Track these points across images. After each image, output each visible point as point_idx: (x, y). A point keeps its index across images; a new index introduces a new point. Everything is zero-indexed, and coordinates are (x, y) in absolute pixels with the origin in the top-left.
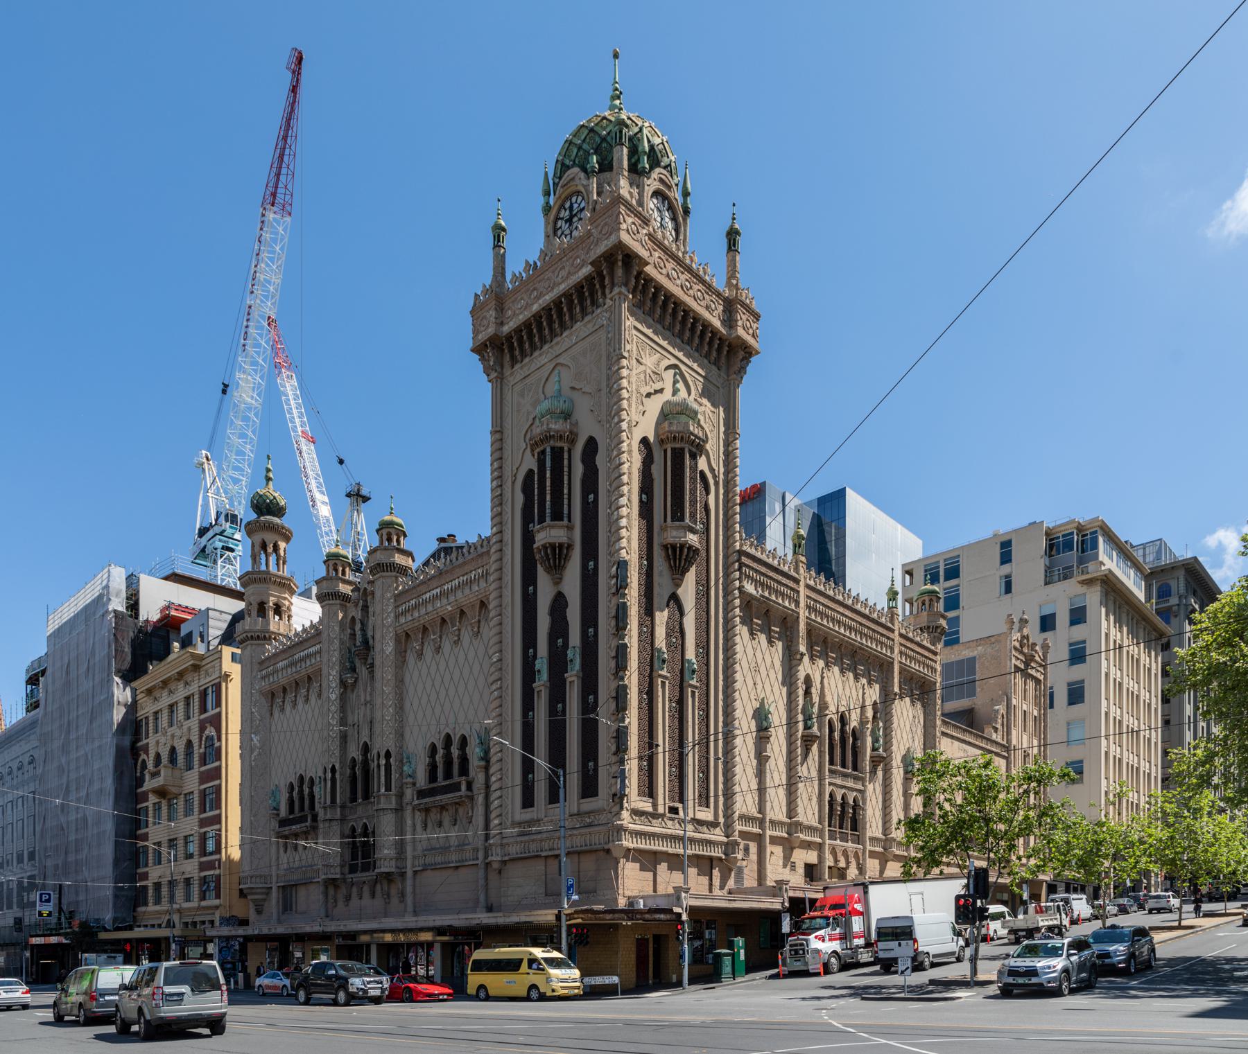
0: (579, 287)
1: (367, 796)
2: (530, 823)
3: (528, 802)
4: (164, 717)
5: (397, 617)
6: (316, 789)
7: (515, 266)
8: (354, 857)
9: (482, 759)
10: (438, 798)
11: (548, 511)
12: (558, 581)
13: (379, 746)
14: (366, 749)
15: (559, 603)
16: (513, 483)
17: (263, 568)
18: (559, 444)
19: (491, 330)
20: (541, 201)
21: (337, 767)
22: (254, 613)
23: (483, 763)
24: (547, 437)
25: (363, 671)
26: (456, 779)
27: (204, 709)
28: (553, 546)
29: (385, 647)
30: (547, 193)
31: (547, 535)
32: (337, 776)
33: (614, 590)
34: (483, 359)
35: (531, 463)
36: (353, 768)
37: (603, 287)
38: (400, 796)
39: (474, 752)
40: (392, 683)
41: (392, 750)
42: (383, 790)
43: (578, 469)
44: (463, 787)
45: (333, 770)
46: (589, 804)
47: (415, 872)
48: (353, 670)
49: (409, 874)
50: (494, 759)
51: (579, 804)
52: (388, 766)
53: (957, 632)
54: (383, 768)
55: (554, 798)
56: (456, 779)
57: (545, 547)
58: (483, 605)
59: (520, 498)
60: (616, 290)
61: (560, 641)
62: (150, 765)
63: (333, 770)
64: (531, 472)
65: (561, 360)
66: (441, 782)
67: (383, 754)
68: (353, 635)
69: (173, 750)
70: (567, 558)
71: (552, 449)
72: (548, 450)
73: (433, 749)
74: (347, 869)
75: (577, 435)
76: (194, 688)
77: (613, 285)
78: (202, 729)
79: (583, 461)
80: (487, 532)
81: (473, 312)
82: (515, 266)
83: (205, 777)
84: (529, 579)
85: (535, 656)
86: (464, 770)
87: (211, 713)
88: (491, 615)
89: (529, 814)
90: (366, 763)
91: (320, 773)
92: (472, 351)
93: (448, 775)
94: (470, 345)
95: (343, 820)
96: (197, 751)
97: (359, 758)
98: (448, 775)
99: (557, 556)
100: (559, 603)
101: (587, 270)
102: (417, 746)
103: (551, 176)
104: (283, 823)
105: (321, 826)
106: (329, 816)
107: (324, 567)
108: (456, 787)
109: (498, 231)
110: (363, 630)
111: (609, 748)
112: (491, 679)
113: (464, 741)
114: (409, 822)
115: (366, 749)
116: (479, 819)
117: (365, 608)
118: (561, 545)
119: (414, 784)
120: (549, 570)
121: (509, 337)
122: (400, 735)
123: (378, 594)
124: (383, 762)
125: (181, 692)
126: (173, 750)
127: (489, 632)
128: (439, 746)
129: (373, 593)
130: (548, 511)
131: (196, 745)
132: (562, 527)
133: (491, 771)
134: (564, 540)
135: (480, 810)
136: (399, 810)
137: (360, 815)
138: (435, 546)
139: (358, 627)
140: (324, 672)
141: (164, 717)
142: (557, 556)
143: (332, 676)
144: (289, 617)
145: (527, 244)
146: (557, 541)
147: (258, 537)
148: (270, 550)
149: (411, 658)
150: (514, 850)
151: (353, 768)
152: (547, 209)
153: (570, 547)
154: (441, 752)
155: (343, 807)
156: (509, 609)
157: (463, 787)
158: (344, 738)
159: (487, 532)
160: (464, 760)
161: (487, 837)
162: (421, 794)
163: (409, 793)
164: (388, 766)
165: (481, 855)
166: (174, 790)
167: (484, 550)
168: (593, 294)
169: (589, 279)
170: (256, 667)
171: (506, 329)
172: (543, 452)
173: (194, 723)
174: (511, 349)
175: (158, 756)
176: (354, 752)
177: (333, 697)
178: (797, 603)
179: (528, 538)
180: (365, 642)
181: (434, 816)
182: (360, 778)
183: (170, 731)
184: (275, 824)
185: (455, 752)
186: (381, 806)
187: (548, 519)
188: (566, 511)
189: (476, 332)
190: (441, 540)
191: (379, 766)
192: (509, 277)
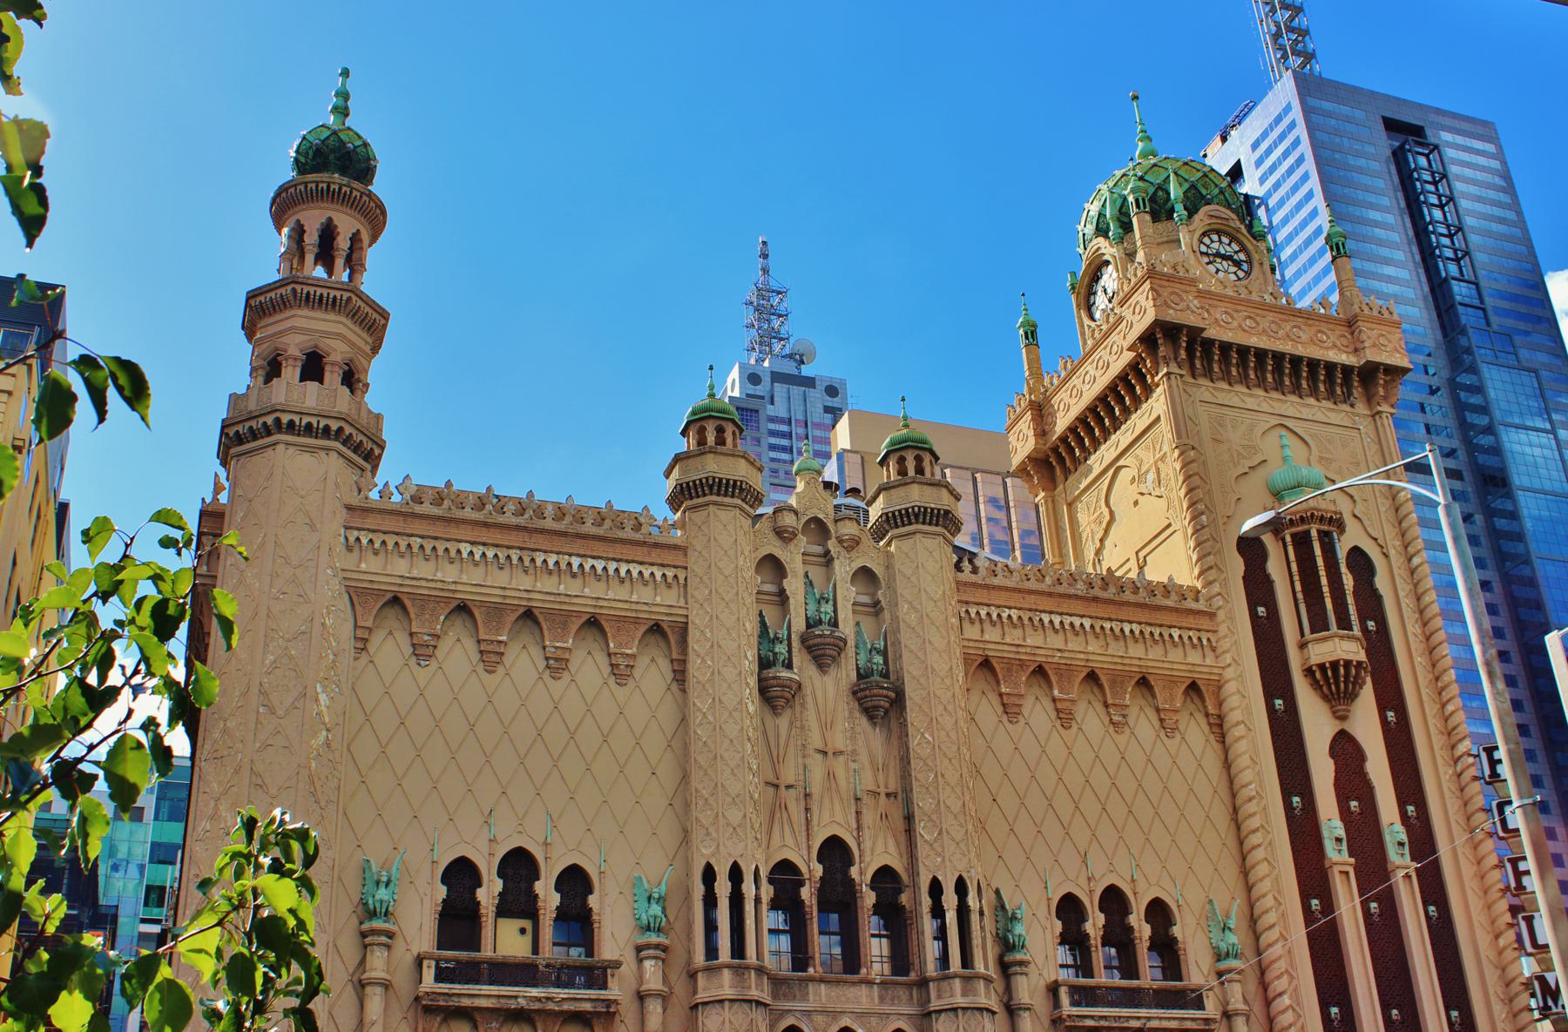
121: (1055, 450)
174: (1061, 460)
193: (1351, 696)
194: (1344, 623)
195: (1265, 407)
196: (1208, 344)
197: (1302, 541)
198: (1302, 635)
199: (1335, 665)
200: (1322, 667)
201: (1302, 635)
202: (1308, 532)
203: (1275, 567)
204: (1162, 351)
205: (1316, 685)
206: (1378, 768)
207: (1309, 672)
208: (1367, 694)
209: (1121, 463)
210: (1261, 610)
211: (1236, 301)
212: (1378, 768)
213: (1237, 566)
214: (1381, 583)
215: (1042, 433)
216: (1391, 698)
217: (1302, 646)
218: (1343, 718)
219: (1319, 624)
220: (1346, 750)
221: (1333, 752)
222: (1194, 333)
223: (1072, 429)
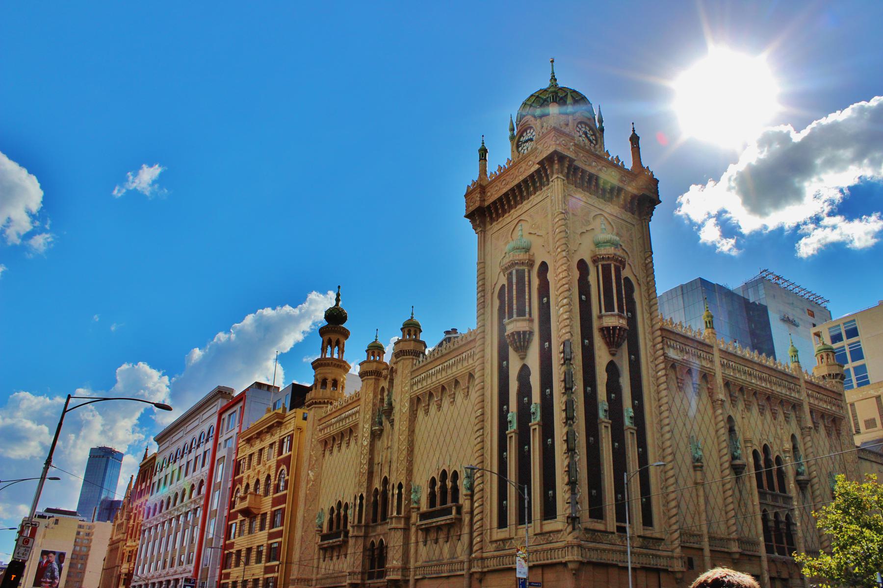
0: (532, 176)
1: (384, 518)
2: (504, 540)
3: (502, 523)
4: (255, 458)
5: (412, 386)
6: (349, 512)
7: (492, 168)
8: (372, 567)
9: (469, 489)
10: (435, 520)
11: (515, 311)
12: (523, 358)
13: (394, 480)
14: (386, 481)
15: (524, 372)
16: (492, 293)
17: (328, 356)
18: (521, 268)
19: (477, 204)
20: (509, 134)
21: (364, 495)
22: (319, 386)
23: (469, 492)
24: (513, 264)
25: (386, 424)
26: (449, 504)
27: (280, 453)
28: (518, 333)
29: (402, 407)
30: (513, 130)
31: (515, 326)
32: (364, 502)
33: (562, 362)
34: (473, 221)
35: (503, 280)
36: (376, 497)
37: (547, 176)
38: (408, 518)
39: (463, 483)
40: (406, 433)
41: (404, 483)
42: (395, 514)
43: (535, 282)
44: (454, 512)
45: (361, 497)
46: (550, 526)
47: (417, 580)
48: (381, 423)
49: (412, 582)
50: (477, 489)
51: (541, 525)
52: (400, 494)
53: (866, 377)
54: (396, 497)
55: (521, 520)
56: (449, 504)
57: (512, 334)
58: (471, 376)
59: (497, 303)
60: (555, 176)
61: (526, 399)
62: (241, 493)
63: (361, 497)
64: (504, 285)
65: (521, 218)
66: (438, 507)
67: (396, 486)
68: (382, 400)
69: (258, 481)
70: (529, 341)
71: (517, 271)
72: (514, 272)
73: (433, 481)
74: (366, 576)
75: (534, 261)
76: (276, 438)
77: (552, 173)
78: (278, 467)
79: (539, 276)
80: (474, 326)
81: (466, 196)
82: (492, 168)
83: (275, 502)
84: (503, 357)
85: (508, 411)
86: (455, 499)
87: (285, 453)
88: (476, 382)
89: (503, 534)
90: (385, 493)
91: (352, 501)
92: (466, 216)
93: (444, 501)
94: (464, 214)
95: (366, 536)
96: (273, 482)
97: (380, 489)
98: (444, 501)
99: (521, 342)
100: (524, 372)
101: (537, 166)
102: (421, 481)
103: (514, 121)
104: (324, 537)
105: (350, 540)
106: (355, 533)
107: (366, 354)
108: (448, 511)
109: (483, 152)
110: (390, 395)
111: (563, 479)
112: (476, 428)
113: (455, 475)
114: (413, 539)
115: (386, 481)
116: (465, 538)
117: (391, 382)
118: (524, 333)
119: (418, 509)
120: (516, 350)
122: (410, 472)
123: (399, 372)
124: (396, 491)
125: (268, 440)
126: (258, 481)
127: (474, 395)
128: (438, 479)
129: (396, 370)
130: (515, 311)
131: (272, 478)
132: (525, 320)
133: (475, 498)
134: (527, 329)
135: (466, 530)
136: (406, 530)
137: (379, 532)
138: (443, 336)
139: (386, 393)
140: (360, 426)
141: (255, 458)
142: (521, 342)
143: (365, 429)
144: (343, 388)
145: (501, 155)
146: (521, 329)
147: (327, 337)
148: (333, 343)
149: (421, 414)
150: (492, 564)
151: (376, 497)
152: (512, 138)
153: (531, 333)
154: (439, 484)
155: (367, 526)
156: (489, 377)
157: (454, 512)
158: (371, 474)
159: (474, 326)
160: (455, 489)
161: (471, 552)
162: (424, 516)
163: (414, 517)
164: (400, 494)
165: (466, 566)
166: (255, 511)
167: (472, 338)
168: (540, 178)
169: (538, 171)
170: (317, 423)
171: (486, 204)
172: (511, 273)
173: (273, 462)
175: (248, 485)
176: (377, 485)
177: (365, 443)
178: (712, 361)
179: (502, 328)
180: (390, 404)
181: (433, 535)
182: (377, 504)
183: (259, 468)
184: (318, 539)
185: (449, 484)
186: (394, 525)
187: (515, 316)
188: (527, 309)
189: (467, 207)
190: (447, 332)
191: (393, 495)
192: (488, 174)
193: (619, 345)
194: (621, 309)
195: (596, 205)
196: (576, 169)
197: (606, 270)
198: (601, 311)
199: (614, 328)
200: (608, 328)
201: (601, 311)
202: (610, 265)
203: (592, 279)
204: (556, 166)
205: (604, 337)
206: (625, 381)
207: (602, 330)
208: (625, 346)
209: (521, 218)
210: (583, 297)
211: (588, 151)
212: (625, 381)
213: (576, 274)
214: (636, 295)
215: (483, 200)
216: (634, 350)
217: (600, 317)
218: (613, 355)
219: (609, 307)
220: (612, 369)
221: (607, 370)
222: (571, 161)
223: (494, 203)
